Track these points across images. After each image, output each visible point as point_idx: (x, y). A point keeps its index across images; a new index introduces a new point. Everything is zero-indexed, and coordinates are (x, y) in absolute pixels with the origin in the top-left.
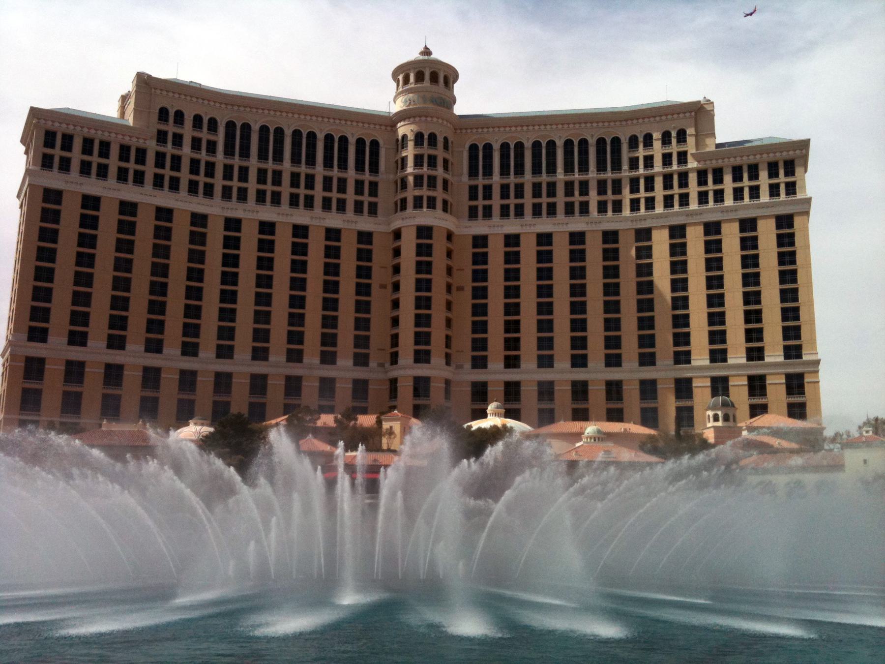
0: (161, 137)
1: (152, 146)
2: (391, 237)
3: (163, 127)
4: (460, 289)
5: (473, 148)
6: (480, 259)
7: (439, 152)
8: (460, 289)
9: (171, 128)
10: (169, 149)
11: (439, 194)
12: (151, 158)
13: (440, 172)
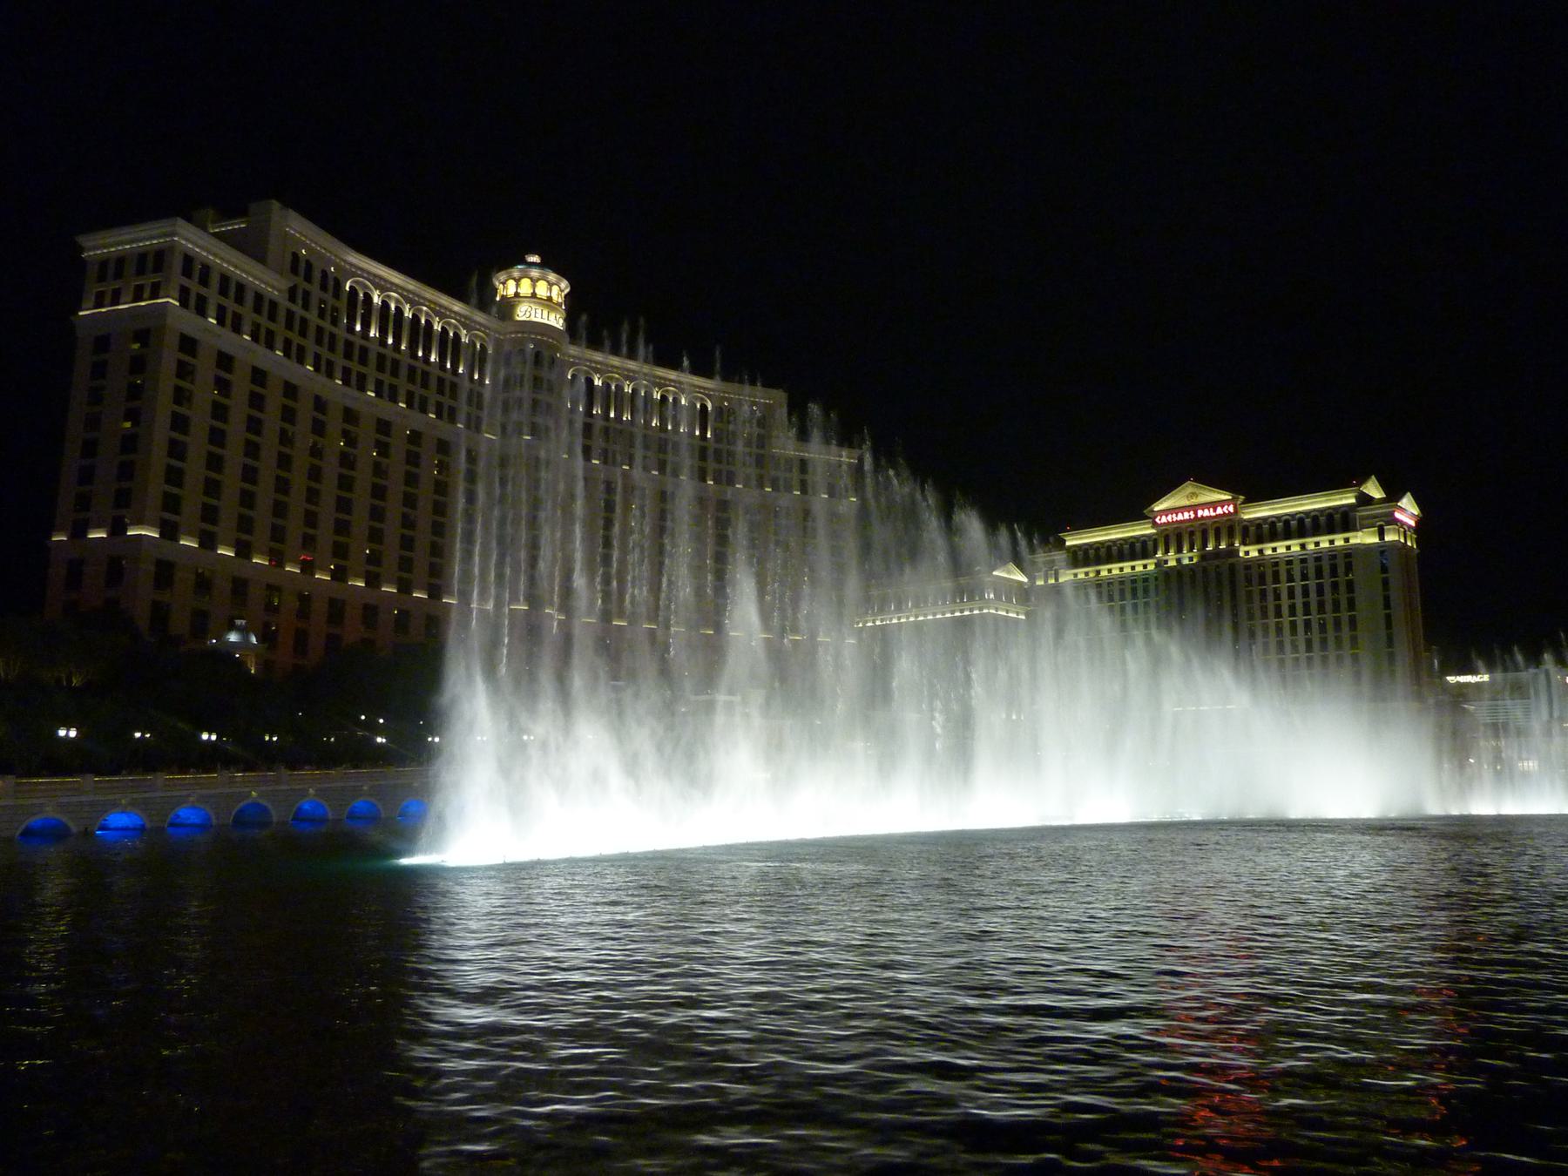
0: (292, 294)
1: (284, 303)
10: (297, 309)
12: (282, 316)
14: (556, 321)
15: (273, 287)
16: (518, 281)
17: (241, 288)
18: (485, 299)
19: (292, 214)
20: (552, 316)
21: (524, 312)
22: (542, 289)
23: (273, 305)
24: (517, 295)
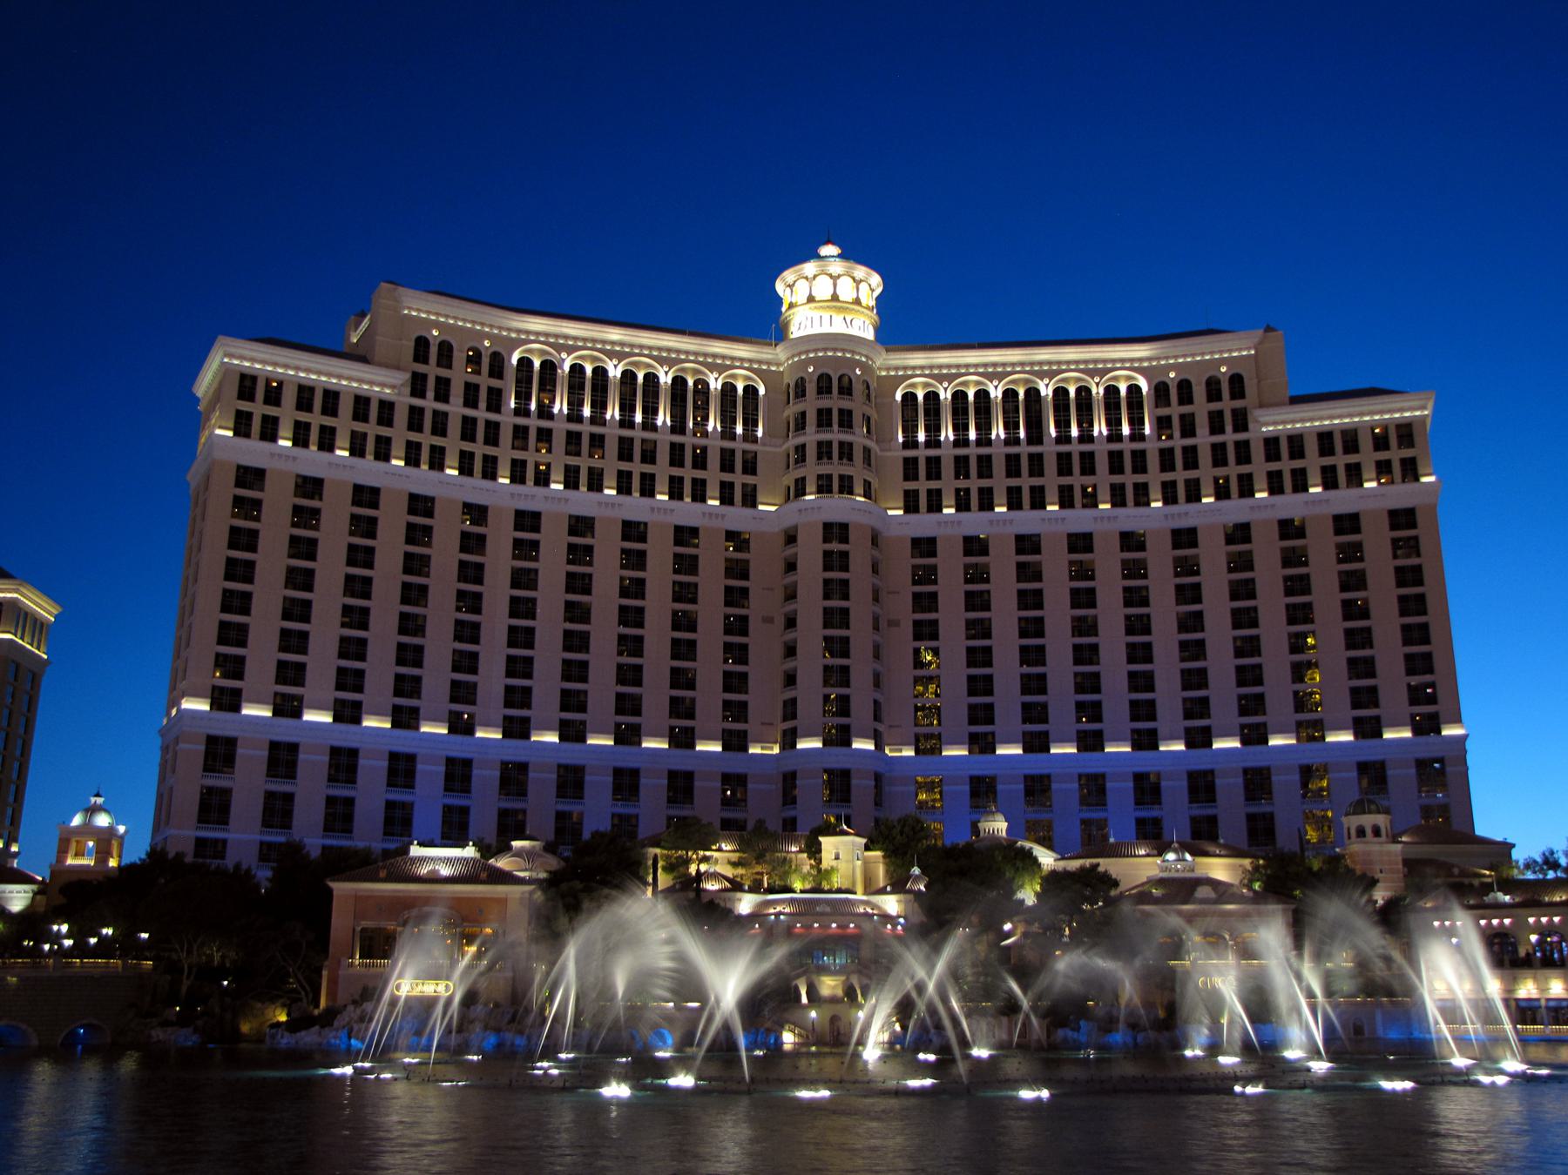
0: (418, 385)
1: (404, 400)
2: (781, 540)
3: (421, 368)
4: (893, 623)
5: (909, 398)
6: (926, 575)
7: (856, 405)
8: (893, 623)
9: (432, 370)
10: (429, 404)
11: (856, 471)
12: (401, 417)
13: (858, 437)
14: (863, 327)
15: (383, 385)
16: (791, 286)
17: (331, 398)
18: (765, 321)
19: (401, 290)
20: (838, 318)
21: (804, 322)
22: (823, 289)
23: (387, 408)
24: (791, 306)
